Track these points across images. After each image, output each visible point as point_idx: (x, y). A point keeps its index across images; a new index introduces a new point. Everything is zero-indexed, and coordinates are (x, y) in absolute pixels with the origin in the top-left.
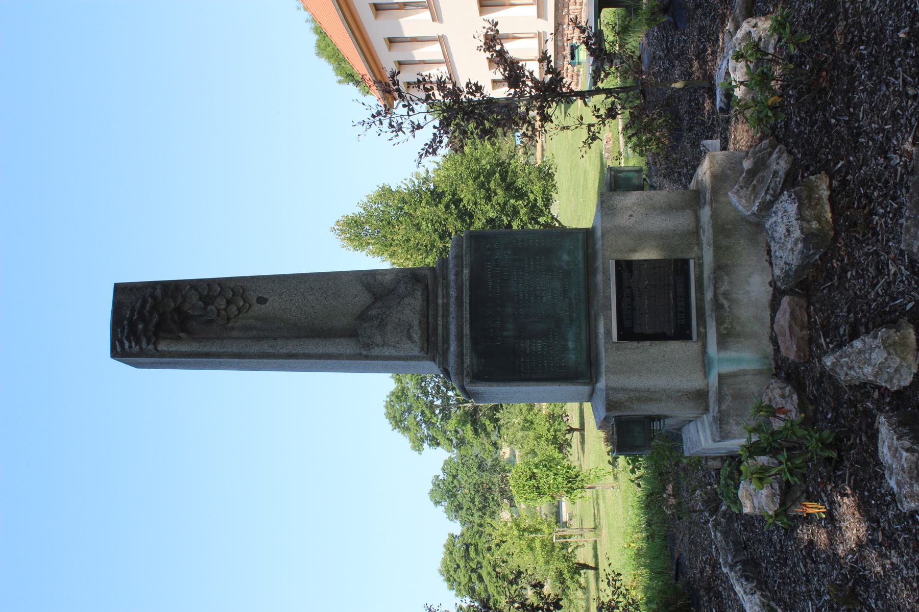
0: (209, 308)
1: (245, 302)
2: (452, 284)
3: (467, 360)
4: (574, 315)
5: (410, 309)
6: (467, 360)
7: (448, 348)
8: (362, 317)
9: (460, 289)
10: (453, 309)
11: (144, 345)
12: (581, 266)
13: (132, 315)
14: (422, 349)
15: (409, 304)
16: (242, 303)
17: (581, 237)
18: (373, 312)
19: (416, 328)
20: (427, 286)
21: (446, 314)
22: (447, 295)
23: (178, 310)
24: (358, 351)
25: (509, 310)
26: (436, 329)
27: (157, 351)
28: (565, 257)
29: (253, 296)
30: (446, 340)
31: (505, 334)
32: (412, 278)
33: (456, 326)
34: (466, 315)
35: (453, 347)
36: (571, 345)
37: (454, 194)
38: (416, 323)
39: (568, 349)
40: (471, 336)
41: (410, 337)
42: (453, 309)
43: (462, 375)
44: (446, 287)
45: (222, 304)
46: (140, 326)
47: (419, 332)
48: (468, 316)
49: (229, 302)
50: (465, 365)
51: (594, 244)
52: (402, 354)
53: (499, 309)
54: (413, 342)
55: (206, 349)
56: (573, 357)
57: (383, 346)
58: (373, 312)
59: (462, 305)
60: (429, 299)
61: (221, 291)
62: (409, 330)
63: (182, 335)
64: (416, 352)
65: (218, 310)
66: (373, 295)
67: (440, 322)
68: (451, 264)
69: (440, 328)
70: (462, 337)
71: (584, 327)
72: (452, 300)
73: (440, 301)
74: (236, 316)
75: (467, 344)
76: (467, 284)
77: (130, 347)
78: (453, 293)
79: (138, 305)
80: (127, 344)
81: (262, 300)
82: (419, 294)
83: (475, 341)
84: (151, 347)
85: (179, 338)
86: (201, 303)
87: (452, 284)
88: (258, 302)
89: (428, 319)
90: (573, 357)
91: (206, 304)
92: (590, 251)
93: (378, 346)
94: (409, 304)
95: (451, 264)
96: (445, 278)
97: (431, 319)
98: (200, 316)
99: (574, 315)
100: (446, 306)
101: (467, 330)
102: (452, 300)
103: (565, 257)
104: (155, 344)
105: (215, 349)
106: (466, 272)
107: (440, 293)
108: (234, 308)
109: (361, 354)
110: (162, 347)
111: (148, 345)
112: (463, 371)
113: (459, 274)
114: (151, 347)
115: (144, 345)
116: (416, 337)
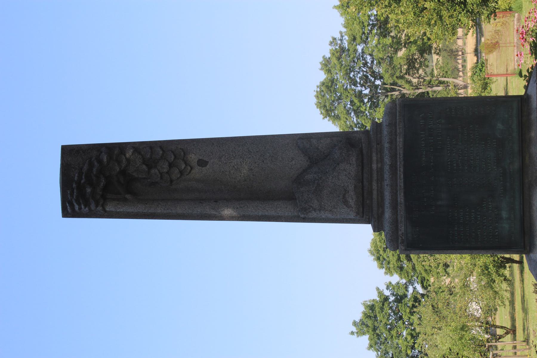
0: (153, 171)
1: (186, 163)
2: (386, 152)
3: (402, 229)
5: (346, 174)
6: (402, 229)
7: (383, 213)
8: (299, 180)
9: (394, 157)
10: (387, 175)
11: (93, 207)
13: (80, 178)
14: (358, 213)
15: (345, 170)
16: (183, 166)
18: (309, 177)
19: (352, 193)
20: (361, 151)
21: (381, 179)
22: (381, 160)
23: (123, 172)
24: (296, 214)
26: (371, 193)
27: (105, 211)
28: (500, 126)
29: (193, 158)
30: (381, 205)
31: (439, 203)
32: (345, 141)
33: (390, 191)
34: (401, 183)
35: (388, 214)
36: (504, 214)
38: (351, 188)
41: (346, 203)
42: (387, 175)
44: (380, 152)
45: (165, 167)
46: (89, 190)
47: (354, 197)
48: (402, 185)
49: (171, 165)
50: (400, 233)
51: (529, 114)
52: (338, 217)
54: (348, 206)
55: (152, 211)
56: (506, 226)
57: (320, 210)
58: (309, 177)
60: (363, 163)
61: (163, 154)
62: (344, 195)
63: (128, 196)
64: (352, 216)
65: (161, 174)
66: (309, 158)
67: (375, 186)
68: (385, 131)
69: (375, 192)
72: (387, 168)
73: (374, 166)
74: (178, 178)
76: (400, 152)
77: (80, 209)
78: (387, 160)
79: (86, 168)
80: (77, 207)
81: (202, 163)
82: (353, 160)
84: (100, 208)
85: (125, 200)
86: (144, 167)
87: (386, 152)
88: (199, 165)
89: (362, 182)
90: (506, 226)
91: (150, 167)
93: (315, 210)
94: (345, 170)
95: (385, 131)
96: (379, 143)
97: (366, 183)
98: (144, 178)
100: (380, 171)
101: (401, 198)
102: (387, 168)
103: (500, 126)
104: (103, 206)
105: (159, 211)
106: (400, 140)
107: (374, 158)
108: (177, 171)
109: (299, 217)
110: (109, 208)
111: (97, 206)
113: (393, 142)
114: (100, 208)
115: (93, 207)
116: (352, 202)
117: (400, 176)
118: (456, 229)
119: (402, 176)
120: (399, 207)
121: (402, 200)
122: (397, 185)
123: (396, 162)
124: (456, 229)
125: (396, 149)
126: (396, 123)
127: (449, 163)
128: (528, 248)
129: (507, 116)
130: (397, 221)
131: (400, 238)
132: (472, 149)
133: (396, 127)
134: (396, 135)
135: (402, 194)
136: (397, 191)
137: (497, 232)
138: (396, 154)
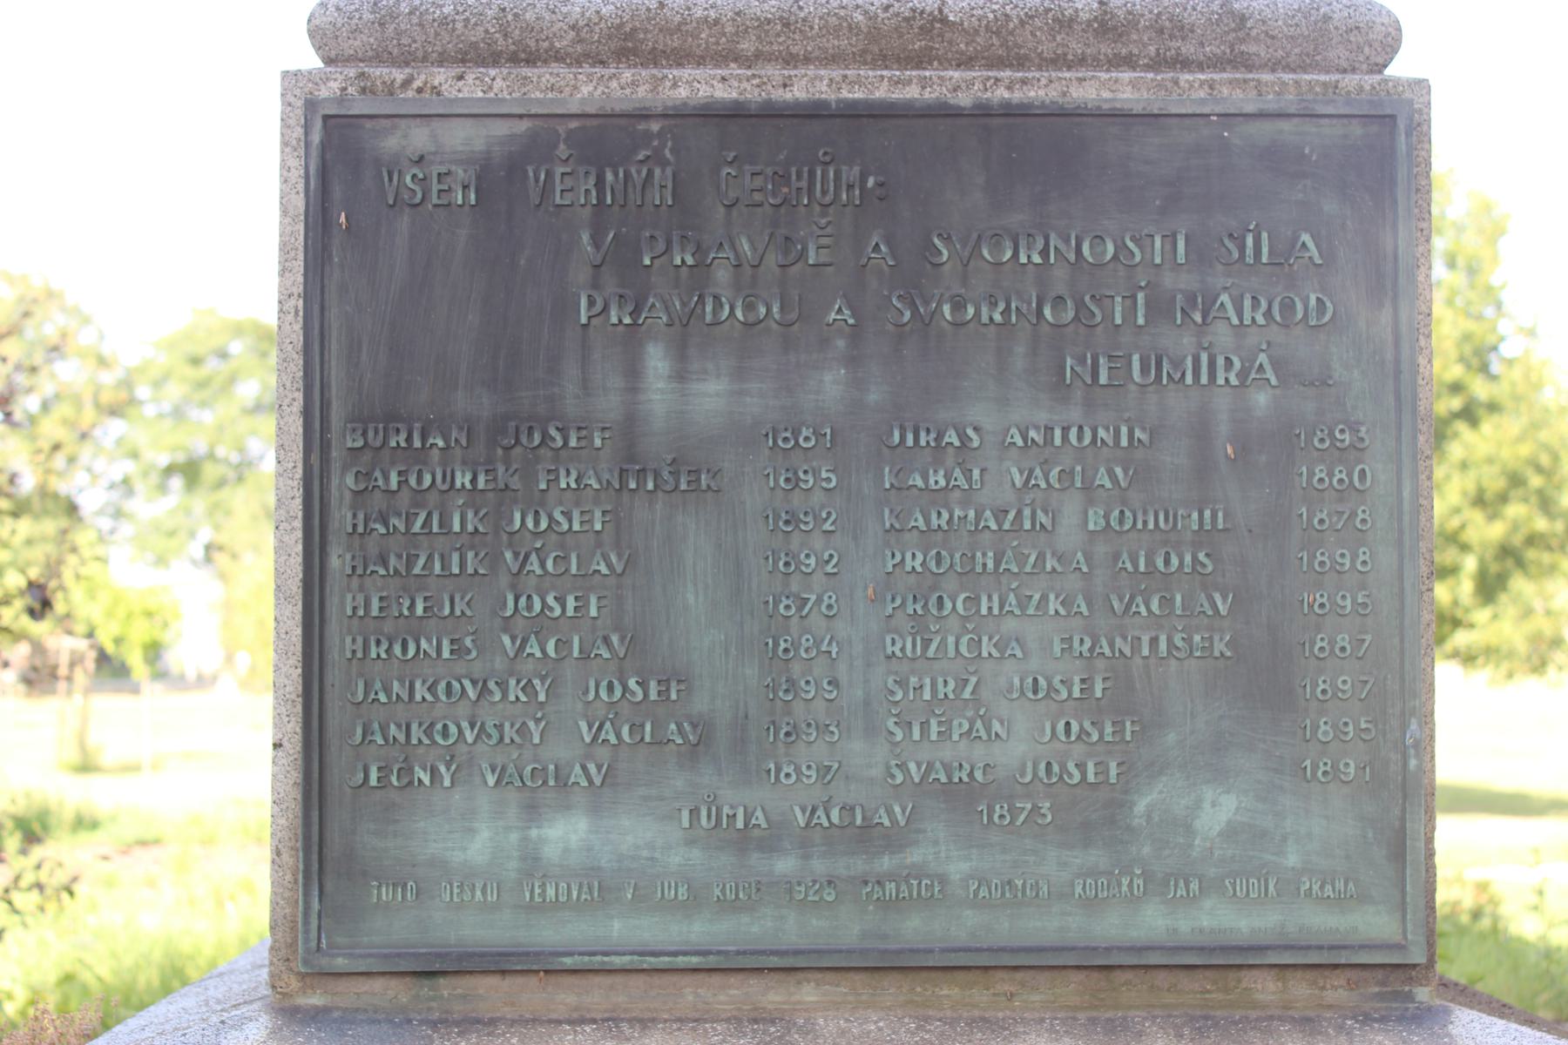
3: (470, 87)
4: (785, 865)
12: (1153, 922)
17: (1373, 923)
25: (830, 386)
28: (1218, 810)
31: (657, 361)
34: (809, 85)
36: (566, 834)
37: (1493, 407)
39: (532, 811)
40: (644, 115)
43: (380, 57)
48: (798, 93)
50: (441, 76)
53: (838, 314)
59: (883, 60)
70: (654, 58)
71: (700, 930)
75: (588, 89)
76: (1041, 89)
83: (605, 139)
92: (1265, 988)
99: (785, 865)
112: (405, 59)
117: (858, 81)
118: (463, 479)
119: (858, 95)
120: (627, 75)
121: (683, 92)
122: (790, 60)
123: (965, 62)
124: (463, 479)
125: (1059, 61)
126: (1241, 62)
127: (952, 437)
128: (316, 1000)
129: (1292, 860)
130: (531, 61)
131: (399, 75)
132: (1053, 605)
133: (1217, 63)
134: (1157, 64)
135: (723, 93)
136: (747, 61)
137: (434, 772)
138: (1021, 63)
